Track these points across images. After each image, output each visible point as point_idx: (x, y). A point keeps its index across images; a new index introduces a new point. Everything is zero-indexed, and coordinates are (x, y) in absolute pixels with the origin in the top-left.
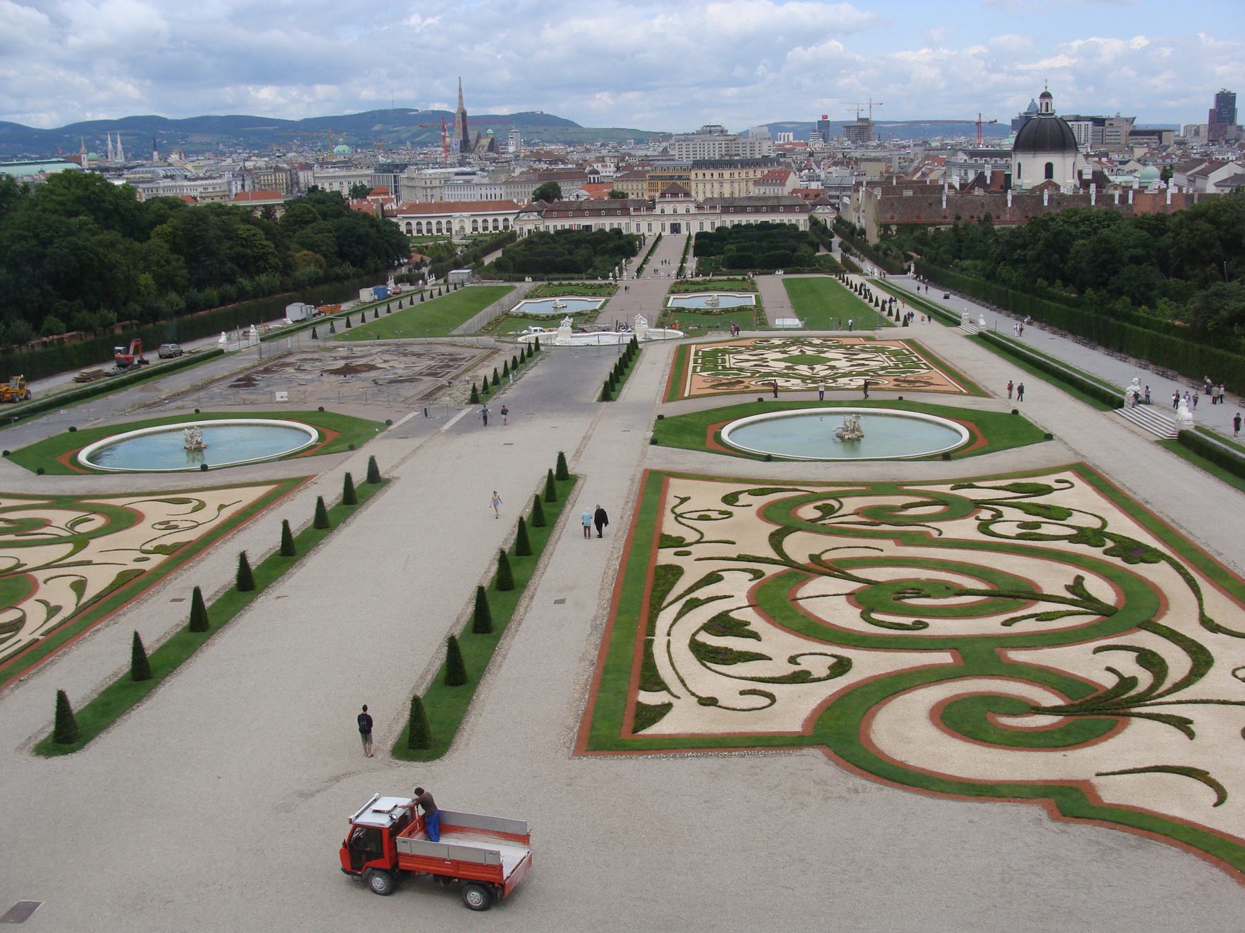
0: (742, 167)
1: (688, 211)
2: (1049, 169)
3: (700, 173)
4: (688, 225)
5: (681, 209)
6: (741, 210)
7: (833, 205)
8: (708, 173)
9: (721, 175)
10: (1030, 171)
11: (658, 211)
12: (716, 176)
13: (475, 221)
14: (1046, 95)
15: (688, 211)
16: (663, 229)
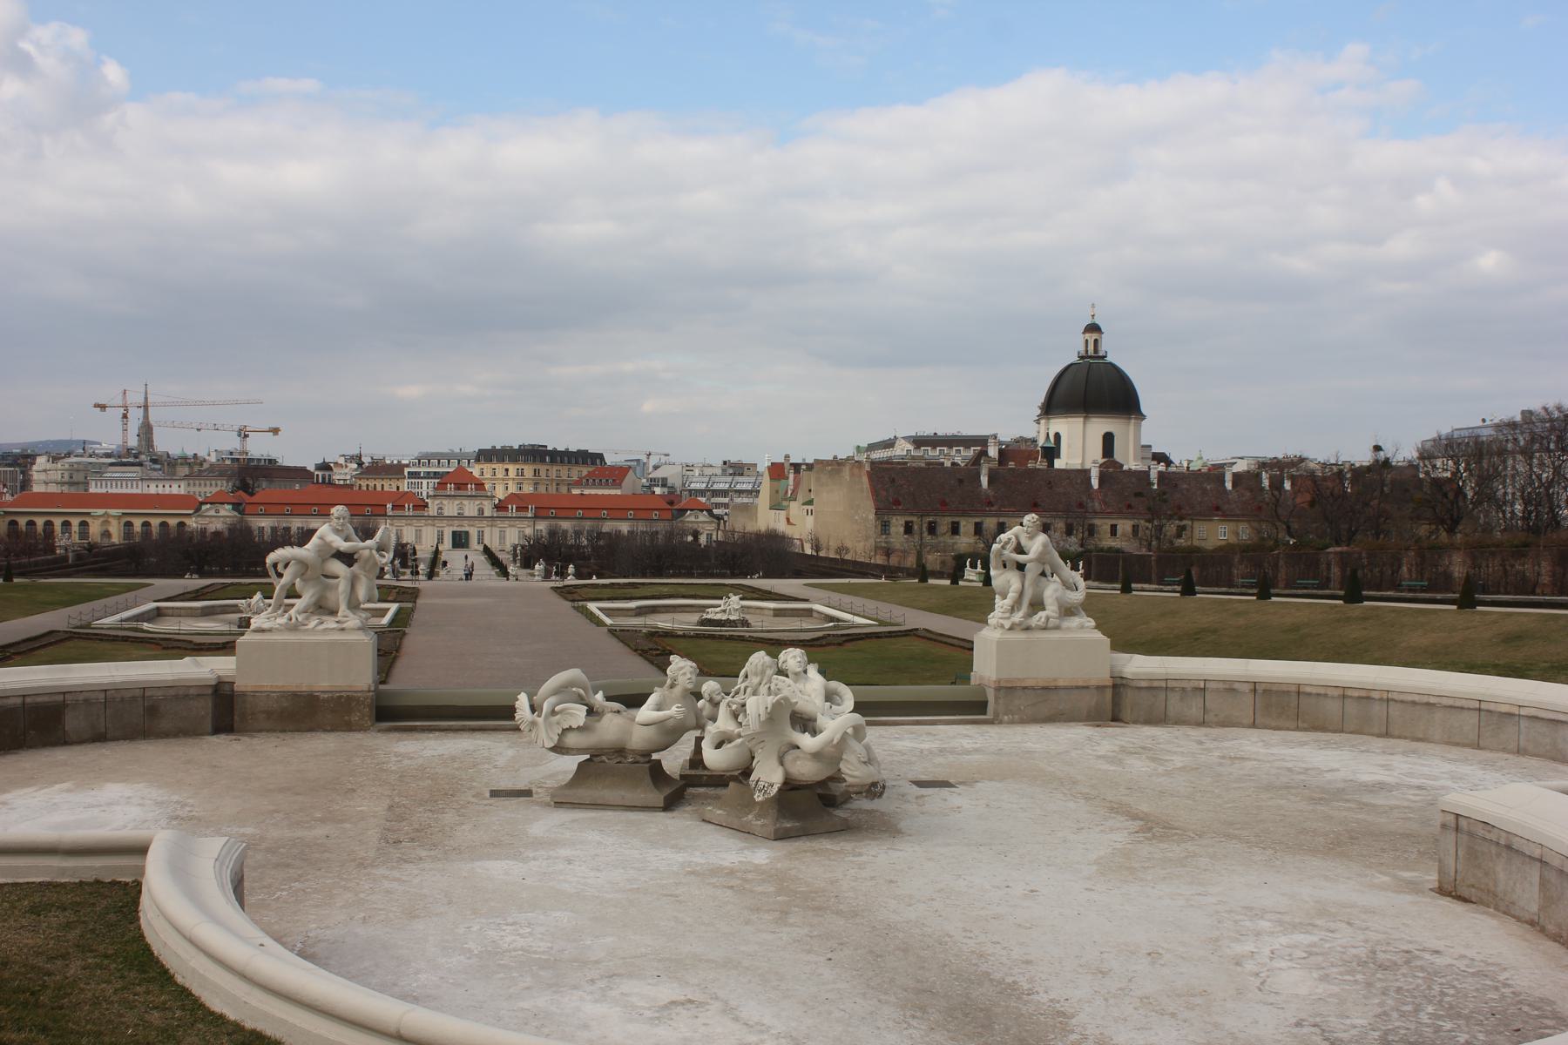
0: (553, 461)
1: (481, 511)
2: (1108, 439)
3: (487, 468)
4: (481, 535)
5: (470, 508)
6: (565, 511)
7: (710, 512)
8: (500, 468)
9: (521, 473)
10: (1079, 443)
11: (432, 510)
12: (512, 473)
13: (129, 524)
14: (1093, 328)
15: (481, 511)
16: (440, 540)
